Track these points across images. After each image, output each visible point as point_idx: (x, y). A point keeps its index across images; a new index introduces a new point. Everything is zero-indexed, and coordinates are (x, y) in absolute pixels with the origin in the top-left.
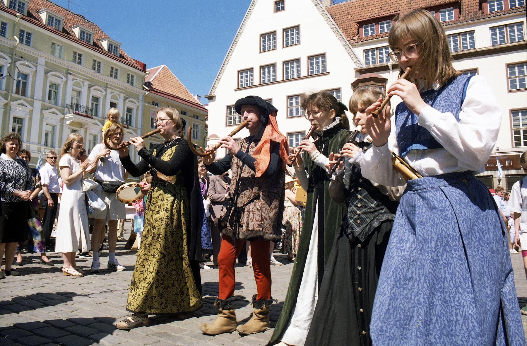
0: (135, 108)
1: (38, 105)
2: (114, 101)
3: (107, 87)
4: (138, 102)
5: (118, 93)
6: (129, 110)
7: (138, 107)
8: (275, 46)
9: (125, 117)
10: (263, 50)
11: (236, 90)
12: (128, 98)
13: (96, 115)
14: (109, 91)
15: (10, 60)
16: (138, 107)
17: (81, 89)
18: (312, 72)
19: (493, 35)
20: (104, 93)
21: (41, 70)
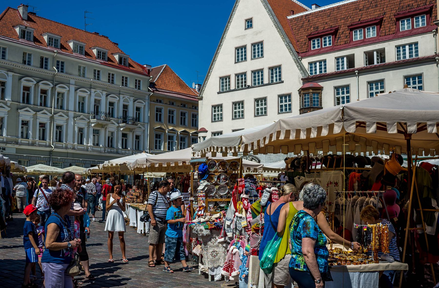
0: (143, 107)
1: (71, 114)
2: (126, 103)
3: (120, 94)
4: (145, 102)
5: (129, 97)
6: (138, 109)
7: (145, 106)
8: (245, 58)
9: (135, 116)
10: (237, 61)
11: (218, 93)
12: (137, 100)
13: (112, 116)
14: (121, 96)
15: (52, 86)
16: (145, 106)
17: (100, 98)
18: (272, 81)
19: (398, 51)
20: (118, 99)
21: (72, 88)
